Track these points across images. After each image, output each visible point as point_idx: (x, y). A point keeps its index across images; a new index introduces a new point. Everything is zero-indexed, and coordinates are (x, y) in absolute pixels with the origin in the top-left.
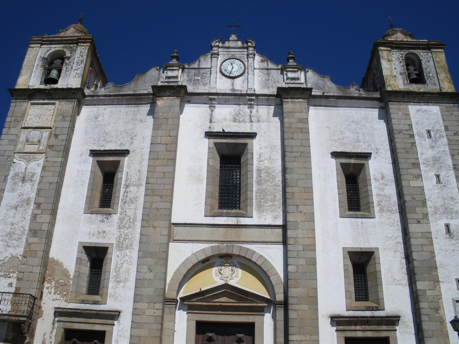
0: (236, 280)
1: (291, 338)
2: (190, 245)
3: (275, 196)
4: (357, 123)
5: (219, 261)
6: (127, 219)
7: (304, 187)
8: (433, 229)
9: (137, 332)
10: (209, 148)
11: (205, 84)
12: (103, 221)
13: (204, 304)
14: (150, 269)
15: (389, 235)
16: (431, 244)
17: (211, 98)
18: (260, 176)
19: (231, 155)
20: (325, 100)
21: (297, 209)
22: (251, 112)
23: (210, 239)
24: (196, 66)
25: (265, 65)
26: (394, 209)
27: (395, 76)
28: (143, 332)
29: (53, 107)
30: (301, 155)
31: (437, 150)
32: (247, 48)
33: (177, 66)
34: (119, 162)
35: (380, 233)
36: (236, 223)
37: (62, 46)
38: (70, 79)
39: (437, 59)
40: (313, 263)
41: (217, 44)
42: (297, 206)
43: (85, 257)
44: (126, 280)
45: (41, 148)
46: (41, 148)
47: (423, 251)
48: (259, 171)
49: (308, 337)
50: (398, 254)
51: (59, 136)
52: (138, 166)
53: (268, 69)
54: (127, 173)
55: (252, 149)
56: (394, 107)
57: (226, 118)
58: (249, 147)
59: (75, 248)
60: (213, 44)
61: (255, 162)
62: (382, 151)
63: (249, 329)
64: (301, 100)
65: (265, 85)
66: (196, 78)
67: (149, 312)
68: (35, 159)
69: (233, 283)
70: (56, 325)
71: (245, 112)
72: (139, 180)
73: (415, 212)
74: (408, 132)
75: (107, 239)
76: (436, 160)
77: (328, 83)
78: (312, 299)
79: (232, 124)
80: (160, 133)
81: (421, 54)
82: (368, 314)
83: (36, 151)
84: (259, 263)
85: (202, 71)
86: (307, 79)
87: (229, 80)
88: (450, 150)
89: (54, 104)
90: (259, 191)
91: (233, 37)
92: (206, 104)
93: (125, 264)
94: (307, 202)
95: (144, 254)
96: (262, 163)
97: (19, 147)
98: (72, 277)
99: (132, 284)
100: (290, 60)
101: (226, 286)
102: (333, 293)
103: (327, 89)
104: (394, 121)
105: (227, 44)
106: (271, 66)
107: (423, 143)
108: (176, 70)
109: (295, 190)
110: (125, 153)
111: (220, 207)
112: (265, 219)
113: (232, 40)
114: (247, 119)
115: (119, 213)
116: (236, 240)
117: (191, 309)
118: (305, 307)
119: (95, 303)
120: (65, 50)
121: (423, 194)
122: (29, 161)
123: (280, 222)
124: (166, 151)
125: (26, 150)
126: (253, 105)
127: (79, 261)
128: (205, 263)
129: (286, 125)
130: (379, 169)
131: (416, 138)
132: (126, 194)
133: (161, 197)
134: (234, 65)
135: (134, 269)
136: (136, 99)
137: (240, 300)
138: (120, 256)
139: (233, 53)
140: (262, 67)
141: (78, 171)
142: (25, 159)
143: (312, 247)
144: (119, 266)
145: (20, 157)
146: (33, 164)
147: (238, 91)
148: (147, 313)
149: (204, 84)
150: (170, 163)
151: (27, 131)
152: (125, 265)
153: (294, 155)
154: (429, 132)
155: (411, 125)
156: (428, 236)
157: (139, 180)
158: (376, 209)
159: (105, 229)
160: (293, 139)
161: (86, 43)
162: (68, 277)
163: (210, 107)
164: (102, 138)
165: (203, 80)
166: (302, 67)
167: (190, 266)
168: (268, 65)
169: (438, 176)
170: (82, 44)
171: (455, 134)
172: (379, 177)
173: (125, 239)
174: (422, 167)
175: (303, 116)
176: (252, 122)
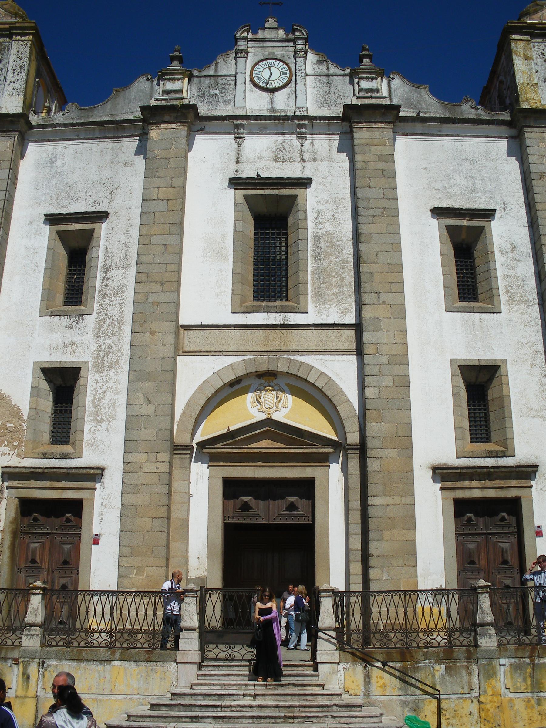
1: (371, 501)
2: (210, 358)
3: (343, 278)
4: (473, 162)
5: (256, 382)
6: (108, 321)
7: (389, 264)
9: (131, 499)
10: (236, 204)
11: (227, 102)
12: (70, 327)
13: (235, 451)
14: (148, 399)
17: (238, 125)
18: (318, 247)
19: (271, 214)
20: (421, 125)
21: (379, 298)
22: (302, 146)
23: (242, 348)
24: (211, 72)
25: (323, 68)
26: (531, 298)
27: (536, 84)
28: (140, 499)
30: (383, 213)
32: (294, 41)
33: (180, 74)
36: (282, 323)
40: (404, 383)
41: (245, 34)
42: (378, 293)
43: (44, 385)
44: (111, 418)
48: (317, 238)
49: (397, 500)
50: (536, 369)
52: (123, 237)
53: (328, 75)
54: (107, 248)
55: (305, 205)
56: (532, 136)
57: (261, 155)
58: (300, 200)
60: (238, 35)
61: (310, 225)
62: (513, 207)
63: (306, 489)
64: (383, 125)
65: (325, 101)
66: (212, 92)
67: (149, 467)
69: (278, 416)
71: (292, 146)
72: (126, 258)
75: (78, 355)
77: (426, 97)
78: (404, 441)
79: (272, 164)
80: (156, 182)
82: (490, 462)
84: (319, 384)
85: (221, 81)
86: (392, 90)
87: (265, 94)
90: (318, 271)
91: (271, 22)
92: (229, 133)
93: (108, 393)
94: (394, 287)
95: (137, 376)
96: (320, 226)
98: (25, 417)
99: (120, 423)
100: (364, 60)
101: (269, 422)
102: (435, 430)
103: (424, 106)
104: (531, 159)
105: (261, 34)
106: (333, 70)
108: (178, 79)
109: (374, 268)
110: (101, 216)
111: (256, 298)
112: (328, 315)
113: (269, 28)
114: (296, 156)
115: (95, 312)
116: (283, 348)
117: (214, 460)
118: (393, 453)
119: (65, 456)
123: (351, 319)
124: (168, 210)
126: (305, 133)
127: (35, 392)
128: (235, 387)
129: (358, 165)
132: (105, 282)
133: (162, 284)
134: (273, 69)
135: (122, 400)
136: (115, 129)
137: (291, 443)
138: (100, 381)
139: (270, 50)
140: (319, 71)
141: (27, 249)
143: (402, 359)
144: (98, 396)
147: (281, 111)
148: (146, 470)
149: (226, 101)
150: (174, 229)
152: (109, 395)
153: (371, 212)
157: (126, 258)
158: (503, 298)
159: (75, 339)
160: (370, 187)
162: (20, 417)
165: (223, 95)
166: (384, 71)
167: (210, 392)
168: (328, 68)
172: (508, 247)
173: (107, 354)
175: (386, 150)
176: (303, 160)
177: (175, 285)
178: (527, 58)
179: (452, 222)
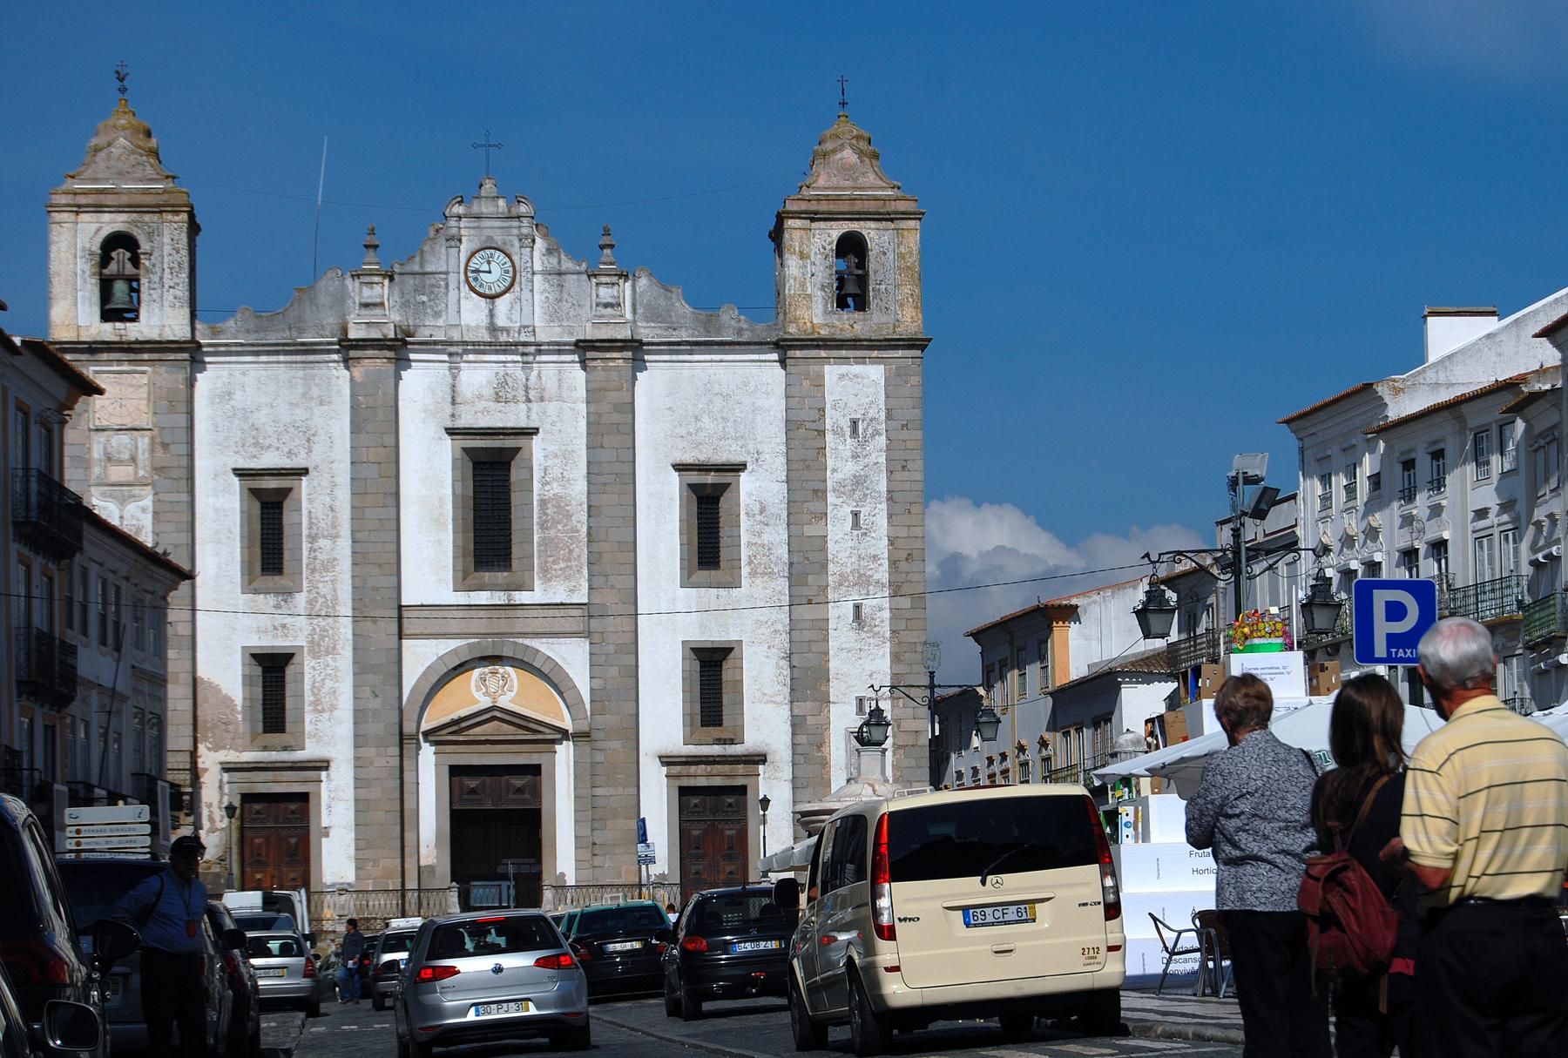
4: (726, 397)
6: (321, 600)
8: (833, 612)
9: (363, 793)
10: (454, 461)
11: (437, 315)
15: (763, 619)
24: (416, 268)
25: (554, 261)
27: (809, 296)
29: (144, 379)
37: (123, 217)
44: (333, 708)
46: (141, 473)
47: (810, 651)
48: (543, 502)
49: (620, 790)
51: (172, 447)
53: (560, 274)
55: (531, 460)
59: (238, 657)
61: (536, 485)
65: (554, 316)
67: (380, 762)
68: (133, 497)
69: (505, 702)
70: (226, 788)
72: (334, 526)
74: (814, 426)
76: (859, 481)
81: (872, 233)
82: (716, 750)
83: (131, 479)
85: (430, 281)
89: (144, 373)
95: (362, 667)
97: (96, 470)
98: (239, 708)
102: (663, 719)
105: (476, 208)
106: (567, 264)
107: (841, 447)
114: (521, 394)
118: (616, 745)
119: (285, 749)
120: (136, 232)
121: (824, 549)
125: (113, 478)
127: (247, 680)
128: (462, 668)
131: (829, 437)
139: (489, 232)
141: (217, 511)
142: (115, 498)
145: (104, 495)
146: (132, 508)
147: (503, 329)
151: (102, 437)
152: (328, 684)
154: (854, 423)
158: (745, 571)
163: (450, 369)
164: (250, 441)
169: (856, 515)
170: (170, 217)
174: (831, 498)
176: (529, 401)
178: (803, 256)
179: (695, 478)
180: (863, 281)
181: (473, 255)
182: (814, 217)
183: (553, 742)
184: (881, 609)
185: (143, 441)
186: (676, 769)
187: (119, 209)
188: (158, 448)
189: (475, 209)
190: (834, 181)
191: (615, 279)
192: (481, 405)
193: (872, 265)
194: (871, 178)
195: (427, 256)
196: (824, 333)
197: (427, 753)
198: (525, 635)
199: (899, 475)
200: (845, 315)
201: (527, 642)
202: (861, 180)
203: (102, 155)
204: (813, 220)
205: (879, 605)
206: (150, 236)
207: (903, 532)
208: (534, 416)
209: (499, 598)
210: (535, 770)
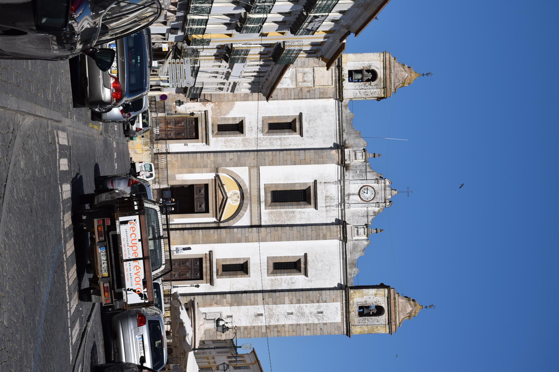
0: (231, 203)
1: (201, 231)
10: (306, 183)
11: (353, 177)
16: (251, 305)
19: (303, 196)
24: (368, 170)
25: (372, 214)
29: (330, 84)
31: (309, 315)
32: (385, 202)
34: (295, 131)
35: (258, 278)
37: (382, 76)
38: (351, 90)
39: (379, 327)
40: (239, 241)
44: (226, 146)
45: (300, 84)
46: (300, 84)
48: (294, 212)
49: (201, 239)
53: (367, 216)
57: (328, 192)
58: (309, 206)
61: (299, 210)
63: (207, 211)
64: (339, 236)
65: (354, 214)
67: (209, 161)
69: (229, 201)
73: (269, 297)
74: (320, 299)
76: (303, 314)
78: (220, 241)
81: (384, 318)
82: (215, 270)
83: (298, 81)
84: (239, 214)
85: (364, 174)
88: (310, 324)
90: (281, 213)
94: (273, 238)
97: (301, 69)
102: (225, 251)
106: (370, 218)
110: (301, 134)
114: (328, 204)
118: (216, 237)
119: (213, 131)
120: (377, 81)
121: (281, 303)
122: (291, 78)
125: (298, 75)
127: (235, 119)
130: (297, 280)
131: (317, 304)
133: (272, 161)
139: (380, 193)
143: (247, 241)
145: (293, 72)
147: (349, 198)
150: (293, 163)
151: (311, 71)
152: (234, 145)
153: (301, 231)
154: (322, 313)
155: (326, 302)
156: (255, 303)
158: (273, 278)
161: (384, 94)
169: (292, 314)
171: (321, 329)
172: (293, 281)
173: (249, 142)
174: (297, 305)
176: (326, 207)
177: (272, 163)
178: (376, 295)
179: (303, 261)
180: (368, 315)
181: (373, 188)
182: (389, 298)
183: (216, 217)
184: (261, 322)
185: (310, 84)
186: (208, 256)
187: (385, 75)
188: (308, 89)
189: (388, 188)
190: (401, 305)
191: (366, 233)
192: (324, 191)
193: (373, 318)
194: (402, 317)
195: (372, 173)
196: (351, 302)
197: (212, 176)
198: (251, 207)
199: (305, 328)
200: (357, 309)
201: (249, 208)
202: (401, 314)
203: (402, 69)
204: (388, 298)
205: (262, 322)
206: (376, 85)
207: (287, 329)
208: (321, 209)
209: (263, 199)
210: (207, 211)
